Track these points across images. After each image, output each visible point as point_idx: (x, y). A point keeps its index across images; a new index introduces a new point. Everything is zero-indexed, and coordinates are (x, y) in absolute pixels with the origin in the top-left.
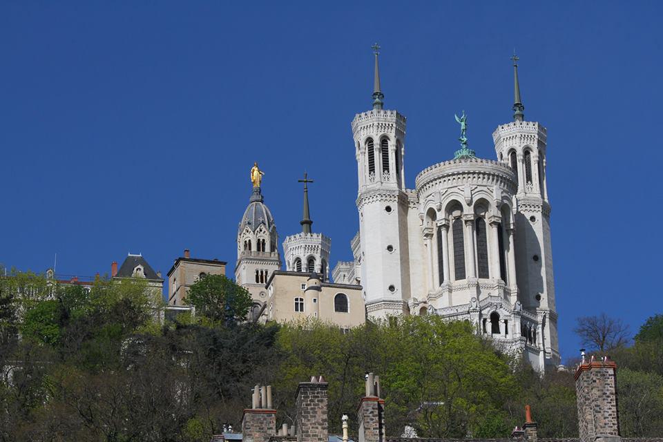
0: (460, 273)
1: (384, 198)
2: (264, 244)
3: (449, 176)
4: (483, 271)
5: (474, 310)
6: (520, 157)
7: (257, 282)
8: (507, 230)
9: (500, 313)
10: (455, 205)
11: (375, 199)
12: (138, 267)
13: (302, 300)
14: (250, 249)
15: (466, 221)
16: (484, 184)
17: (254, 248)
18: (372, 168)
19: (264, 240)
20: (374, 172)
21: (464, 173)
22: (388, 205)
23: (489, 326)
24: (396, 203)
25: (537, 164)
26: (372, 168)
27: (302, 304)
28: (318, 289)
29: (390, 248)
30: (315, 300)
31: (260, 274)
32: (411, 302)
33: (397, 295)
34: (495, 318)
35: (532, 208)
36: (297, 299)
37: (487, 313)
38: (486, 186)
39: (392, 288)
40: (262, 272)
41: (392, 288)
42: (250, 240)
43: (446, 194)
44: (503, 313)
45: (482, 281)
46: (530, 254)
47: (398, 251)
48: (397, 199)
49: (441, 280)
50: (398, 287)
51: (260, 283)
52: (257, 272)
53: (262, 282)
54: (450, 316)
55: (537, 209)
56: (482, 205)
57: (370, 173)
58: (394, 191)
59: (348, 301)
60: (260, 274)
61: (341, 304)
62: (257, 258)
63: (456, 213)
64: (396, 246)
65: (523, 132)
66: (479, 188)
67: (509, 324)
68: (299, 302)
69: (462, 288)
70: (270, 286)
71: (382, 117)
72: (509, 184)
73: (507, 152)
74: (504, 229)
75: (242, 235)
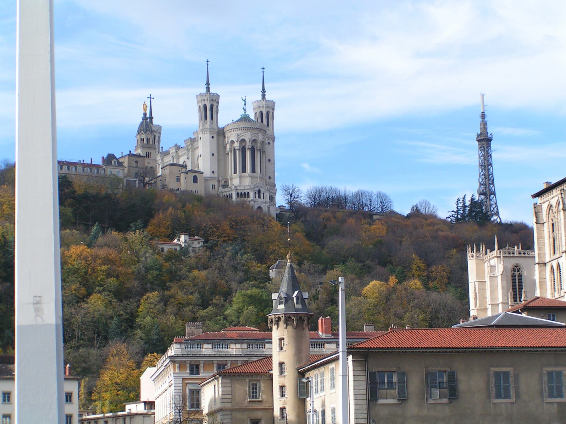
0: (244, 170)
1: (211, 132)
3: (241, 128)
4: (253, 170)
5: (252, 189)
6: (264, 116)
8: (262, 152)
10: (243, 140)
11: (207, 132)
17: (145, 142)
18: (206, 118)
23: (257, 195)
24: (216, 135)
26: (206, 118)
27: (179, 179)
29: (213, 155)
31: (148, 153)
32: (221, 178)
33: (215, 175)
34: (259, 191)
37: (257, 189)
41: (213, 172)
42: (143, 138)
44: (262, 190)
45: (254, 174)
47: (216, 156)
48: (216, 133)
49: (235, 172)
52: (147, 153)
54: (241, 190)
56: (254, 141)
58: (215, 129)
59: (198, 178)
60: (148, 153)
61: (195, 180)
66: (254, 135)
67: (265, 194)
68: (178, 178)
74: (261, 151)
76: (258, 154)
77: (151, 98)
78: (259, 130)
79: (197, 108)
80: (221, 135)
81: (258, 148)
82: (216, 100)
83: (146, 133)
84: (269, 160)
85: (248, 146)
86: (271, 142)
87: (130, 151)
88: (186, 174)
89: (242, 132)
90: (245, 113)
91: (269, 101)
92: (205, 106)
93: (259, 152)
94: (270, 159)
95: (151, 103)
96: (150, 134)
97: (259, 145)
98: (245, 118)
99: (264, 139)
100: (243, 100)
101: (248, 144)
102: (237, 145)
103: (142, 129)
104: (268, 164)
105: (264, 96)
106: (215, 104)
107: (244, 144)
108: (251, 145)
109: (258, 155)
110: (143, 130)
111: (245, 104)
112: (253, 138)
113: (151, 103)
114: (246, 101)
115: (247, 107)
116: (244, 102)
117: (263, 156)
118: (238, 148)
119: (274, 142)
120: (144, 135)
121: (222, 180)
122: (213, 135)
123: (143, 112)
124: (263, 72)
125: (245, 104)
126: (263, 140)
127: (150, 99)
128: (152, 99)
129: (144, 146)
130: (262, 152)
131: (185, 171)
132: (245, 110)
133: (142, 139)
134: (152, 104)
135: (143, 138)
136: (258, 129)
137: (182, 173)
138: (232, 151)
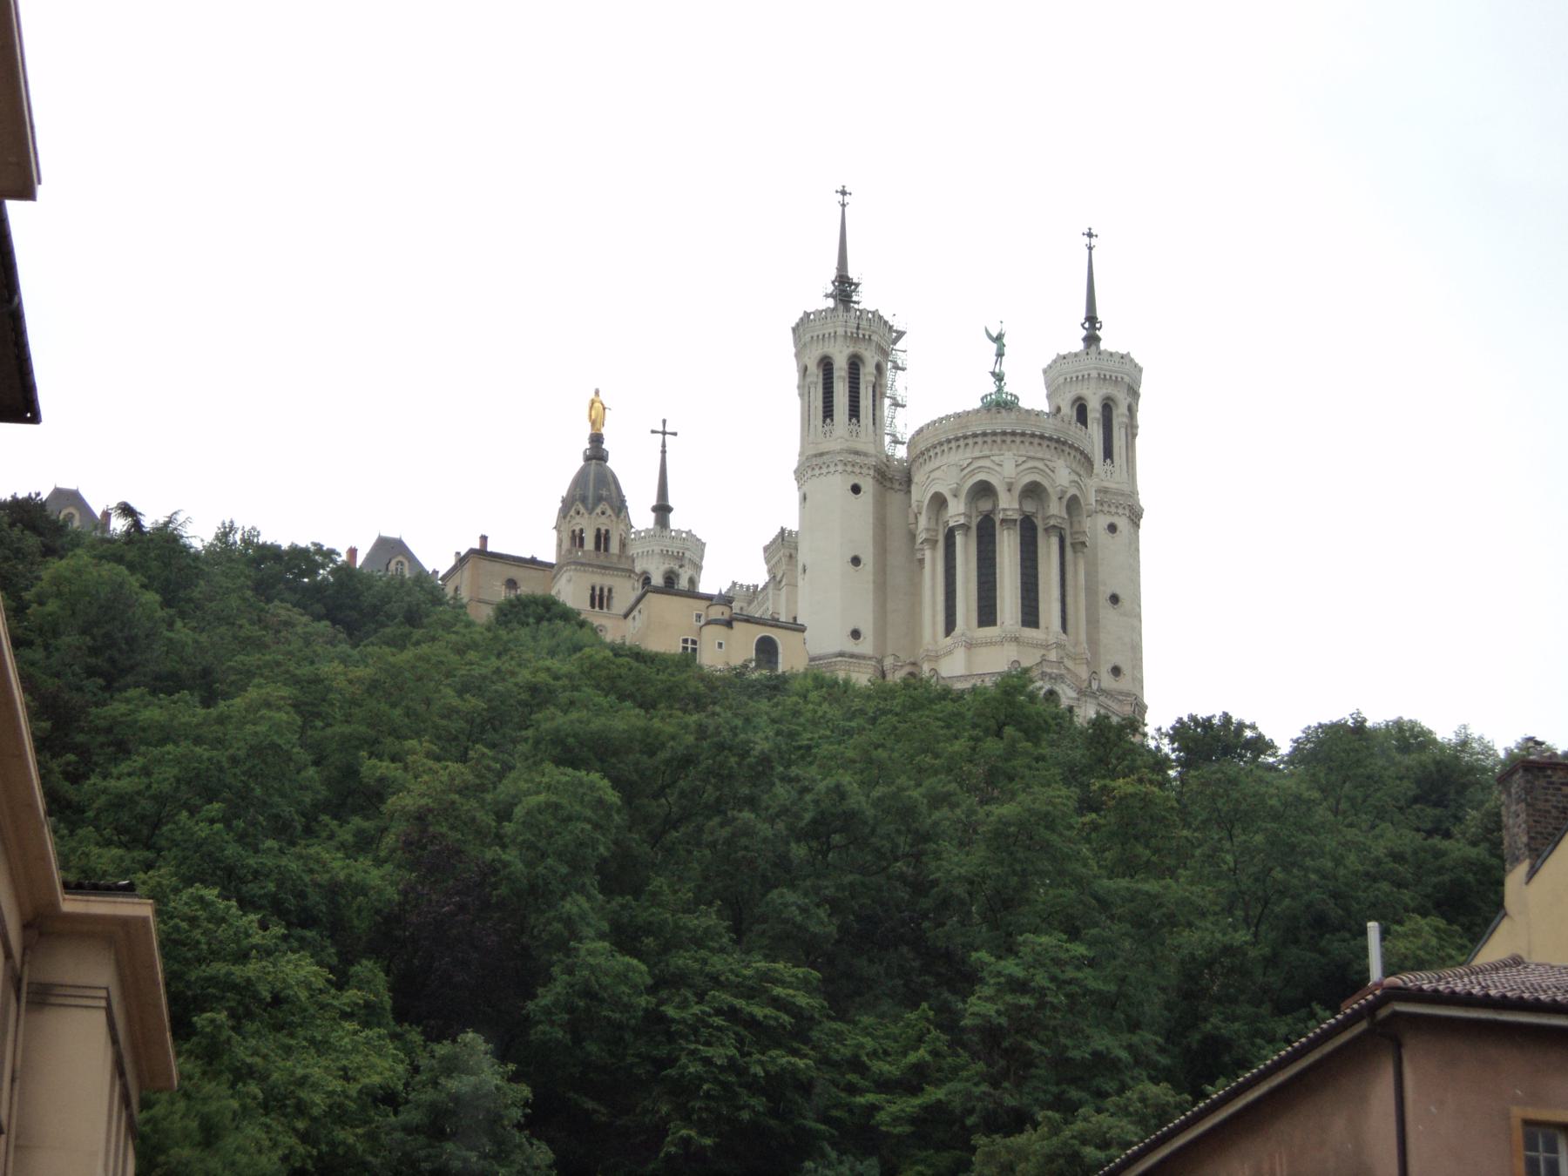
0: (987, 615)
1: (849, 468)
2: (607, 539)
3: (975, 435)
4: (1030, 616)
7: (593, 606)
8: (1072, 544)
9: (1060, 692)
10: (984, 490)
11: (832, 469)
12: (397, 560)
13: (694, 642)
14: (581, 545)
15: (1003, 521)
16: (1040, 455)
17: (589, 544)
18: (828, 412)
19: (607, 531)
20: (832, 420)
21: (1004, 433)
22: (856, 481)
25: (1123, 431)
26: (828, 412)
28: (729, 624)
29: (856, 561)
30: (720, 645)
31: (597, 592)
32: (888, 662)
33: (866, 646)
35: (1113, 510)
36: (685, 641)
38: (1042, 459)
39: (856, 634)
40: (602, 590)
41: (856, 634)
43: (969, 469)
45: (1029, 633)
46: (1105, 592)
48: (872, 472)
50: (867, 630)
51: (597, 609)
52: (593, 589)
53: (601, 607)
55: (1120, 511)
56: (1034, 491)
57: (824, 422)
59: (780, 650)
60: (597, 592)
62: (595, 562)
63: (985, 506)
64: (868, 559)
65: (1101, 369)
66: (1030, 464)
68: (689, 645)
69: (989, 643)
70: (635, 613)
71: (853, 320)
72: (1083, 460)
73: (1070, 402)
74: (1068, 542)
75: (568, 518)
76: (1049, 547)
77: (664, 433)
78: (1053, 445)
79: (793, 376)
80: (897, 486)
81: (1052, 522)
82: (874, 338)
83: (593, 509)
84: (1115, 599)
85: (1005, 510)
86: (1122, 523)
87: (484, 539)
88: (722, 630)
89: (977, 454)
90: (1000, 389)
91: (1111, 354)
92: (826, 365)
93: (1055, 541)
94: (1118, 592)
95: (664, 452)
96: (609, 512)
97: (1056, 509)
98: (1001, 404)
99: (1080, 488)
100: (990, 336)
101: (1008, 504)
102: (956, 511)
103: (578, 492)
104: (1107, 613)
105: (1092, 339)
106: (870, 358)
107: (985, 506)
108: (1017, 506)
109: (1049, 553)
110: (584, 500)
111: (1000, 355)
112: (1027, 479)
113: (664, 452)
114: (1005, 341)
115: (1007, 366)
116: (994, 346)
117: (1076, 565)
118: (962, 520)
119: (1138, 526)
120: (586, 515)
121: (895, 668)
122: (856, 481)
123: (587, 431)
124: (1090, 248)
125: (1000, 355)
126: (1073, 491)
127: (661, 436)
128: (667, 436)
129: (583, 560)
130: (1071, 544)
131: (720, 617)
132: (999, 377)
133: (577, 532)
134: (667, 455)
135: (582, 531)
136: (1050, 439)
137: (708, 623)
138: (937, 541)
